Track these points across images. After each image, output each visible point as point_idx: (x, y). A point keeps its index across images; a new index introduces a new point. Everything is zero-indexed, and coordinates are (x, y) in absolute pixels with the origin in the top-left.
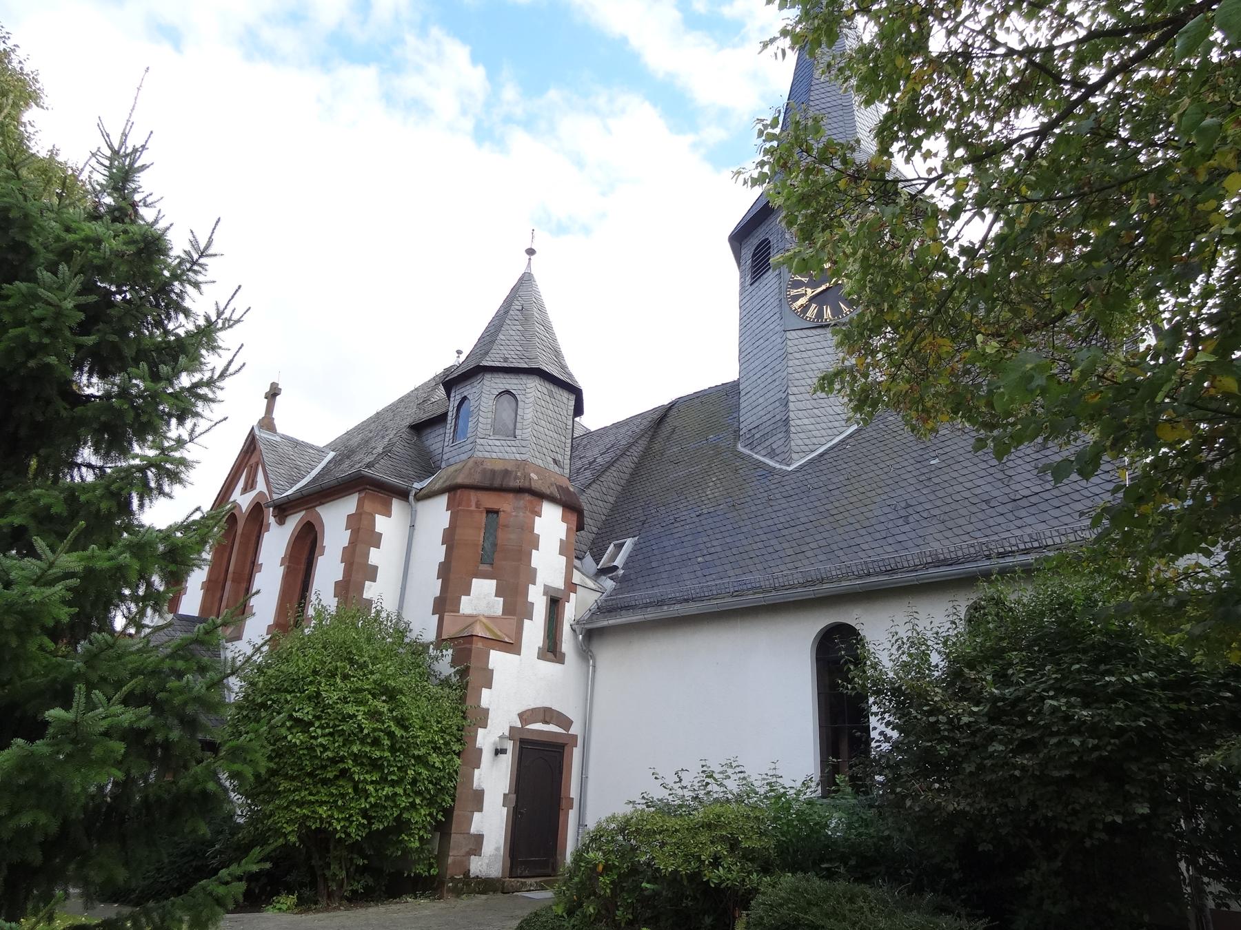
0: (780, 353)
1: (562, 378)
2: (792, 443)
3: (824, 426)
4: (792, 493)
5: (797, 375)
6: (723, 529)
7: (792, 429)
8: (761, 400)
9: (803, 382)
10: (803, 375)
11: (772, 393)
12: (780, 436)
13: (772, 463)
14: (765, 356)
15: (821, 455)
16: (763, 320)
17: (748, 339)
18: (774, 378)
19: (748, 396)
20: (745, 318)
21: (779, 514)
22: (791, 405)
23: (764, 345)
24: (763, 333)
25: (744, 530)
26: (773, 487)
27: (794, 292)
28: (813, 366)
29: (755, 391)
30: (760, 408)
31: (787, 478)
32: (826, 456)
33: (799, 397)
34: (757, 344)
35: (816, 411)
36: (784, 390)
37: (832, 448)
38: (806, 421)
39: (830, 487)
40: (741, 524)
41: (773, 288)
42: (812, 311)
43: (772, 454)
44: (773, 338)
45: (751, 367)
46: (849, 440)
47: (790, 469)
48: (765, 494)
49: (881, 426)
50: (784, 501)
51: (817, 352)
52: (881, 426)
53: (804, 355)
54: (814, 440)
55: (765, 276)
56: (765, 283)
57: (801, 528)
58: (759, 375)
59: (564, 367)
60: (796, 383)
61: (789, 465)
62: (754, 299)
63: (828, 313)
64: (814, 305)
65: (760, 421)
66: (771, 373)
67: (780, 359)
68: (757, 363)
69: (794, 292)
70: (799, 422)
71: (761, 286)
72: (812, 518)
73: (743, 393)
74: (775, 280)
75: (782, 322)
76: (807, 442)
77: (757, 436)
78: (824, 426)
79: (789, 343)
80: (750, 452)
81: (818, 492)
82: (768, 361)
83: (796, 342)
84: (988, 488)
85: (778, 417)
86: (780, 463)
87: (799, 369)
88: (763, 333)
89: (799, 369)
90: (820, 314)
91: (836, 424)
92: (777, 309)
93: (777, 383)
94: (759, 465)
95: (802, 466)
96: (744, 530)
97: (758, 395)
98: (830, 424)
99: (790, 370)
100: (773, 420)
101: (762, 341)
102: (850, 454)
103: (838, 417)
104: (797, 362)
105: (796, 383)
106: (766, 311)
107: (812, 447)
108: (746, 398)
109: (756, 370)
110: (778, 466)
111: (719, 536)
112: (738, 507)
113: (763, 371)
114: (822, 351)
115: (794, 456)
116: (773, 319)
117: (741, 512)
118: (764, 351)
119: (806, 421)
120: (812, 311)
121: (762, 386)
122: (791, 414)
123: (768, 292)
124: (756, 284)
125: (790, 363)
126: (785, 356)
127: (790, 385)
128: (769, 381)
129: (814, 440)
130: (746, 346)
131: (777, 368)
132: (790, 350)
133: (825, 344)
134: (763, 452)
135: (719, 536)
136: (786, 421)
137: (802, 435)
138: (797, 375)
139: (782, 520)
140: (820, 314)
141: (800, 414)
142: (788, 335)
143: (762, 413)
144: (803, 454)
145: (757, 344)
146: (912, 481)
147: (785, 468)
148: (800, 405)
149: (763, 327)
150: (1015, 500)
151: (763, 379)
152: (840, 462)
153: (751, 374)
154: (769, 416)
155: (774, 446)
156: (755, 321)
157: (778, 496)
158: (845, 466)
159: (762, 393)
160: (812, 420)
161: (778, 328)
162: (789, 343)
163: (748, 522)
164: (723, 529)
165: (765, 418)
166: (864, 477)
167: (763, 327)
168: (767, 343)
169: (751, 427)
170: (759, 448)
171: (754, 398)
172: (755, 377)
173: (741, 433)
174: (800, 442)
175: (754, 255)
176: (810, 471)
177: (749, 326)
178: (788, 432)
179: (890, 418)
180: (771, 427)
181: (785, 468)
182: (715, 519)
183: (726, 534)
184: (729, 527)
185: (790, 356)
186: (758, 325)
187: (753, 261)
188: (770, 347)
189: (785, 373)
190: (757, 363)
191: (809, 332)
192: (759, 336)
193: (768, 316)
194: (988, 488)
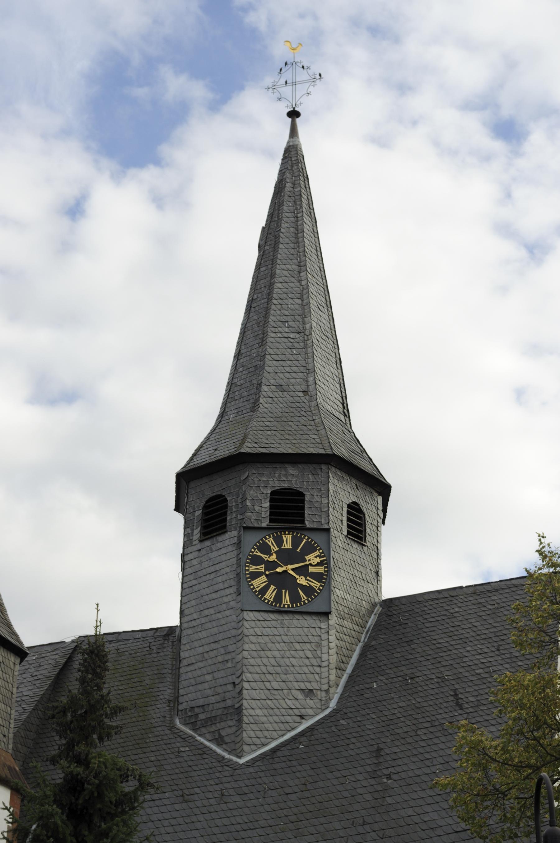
0: (234, 632)
1: (10, 639)
2: (244, 734)
3: (275, 718)
4: (246, 790)
5: (252, 661)
6: (173, 822)
7: (245, 718)
8: (208, 678)
9: (258, 669)
10: (259, 661)
11: (222, 674)
12: (230, 723)
13: (219, 751)
14: (216, 630)
15: (274, 751)
16: (216, 588)
17: (193, 603)
18: (227, 657)
19: (191, 668)
20: (191, 577)
21: (235, 813)
22: (245, 692)
23: (214, 617)
24: (214, 603)
25: (198, 825)
26: (224, 780)
27: (252, 569)
28: (269, 654)
29: (201, 665)
30: (206, 686)
31: (238, 772)
32: (279, 754)
33: (253, 685)
34: (206, 612)
35: (269, 702)
36: (238, 674)
37: (283, 745)
38: (259, 712)
39: (288, 790)
40: (194, 819)
41: (228, 556)
42: (270, 594)
43: (220, 741)
44: (228, 613)
45: (196, 636)
46: (303, 739)
47: (242, 761)
48: (217, 788)
49: (334, 729)
50: (237, 798)
51: (274, 639)
52: (334, 729)
53: (260, 640)
54: (266, 734)
55: (220, 538)
56: (219, 545)
57: (261, 832)
58: (207, 648)
59: (9, 625)
60: (251, 669)
61: (240, 757)
62: (203, 559)
63: (286, 599)
64: (272, 587)
65: (206, 701)
66: (222, 651)
67: (234, 640)
68: (204, 634)
69: (252, 569)
70: (252, 712)
71: (214, 548)
72: (271, 822)
73: (184, 662)
74: (230, 548)
75: (239, 598)
76: (259, 734)
77: (202, 716)
78: (275, 718)
79: (245, 623)
80: (191, 732)
81: (274, 793)
82: (221, 637)
83: (253, 624)
84: (435, 816)
85: (229, 703)
86: (230, 753)
87: (254, 654)
88: (214, 603)
89: (254, 654)
90: (278, 598)
91: (289, 719)
92: (233, 583)
93: (230, 665)
94: (204, 751)
95: (254, 760)
96: (198, 825)
97: (204, 671)
98: (282, 718)
99: (245, 654)
100: (222, 705)
101: (212, 611)
102: (304, 756)
103: (290, 712)
104: (253, 646)
105: (251, 669)
106: (220, 579)
107: (263, 740)
108: (188, 669)
109: (203, 641)
110: (227, 756)
111: (170, 830)
112: (186, 797)
113: (214, 646)
114: (278, 638)
115: (246, 748)
116: (227, 591)
117: (191, 805)
118: (214, 624)
119: (259, 712)
120: (270, 594)
121: (210, 662)
122: (245, 703)
123: (224, 558)
124: (207, 543)
125: (246, 647)
126: (240, 638)
127: (245, 671)
128: (220, 659)
129: (266, 734)
130: (192, 610)
131: (231, 648)
132: (246, 632)
133: (281, 631)
134: (207, 735)
135: (170, 830)
136: (239, 711)
137: (254, 727)
138: (252, 661)
139: (239, 820)
140: (278, 598)
141: (254, 704)
142: (246, 615)
143: (210, 692)
144: (254, 747)
145: (206, 612)
146: (368, 797)
147: (235, 759)
148: (254, 694)
149: (214, 596)
150: (457, 832)
151: (212, 654)
152: (295, 763)
153: (196, 644)
154: (218, 698)
155: (223, 733)
156: (204, 585)
157: (232, 792)
158: (300, 768)
159: (209, 669)
160: (265, 711)
161: (233, 604)
162: (245, 623)
163: (201, 818)
164: (173, 822)
165: (213, 699)
166: (321, 784)
167: (214, 596)
168: (219, 616)
169: (193, 704)
170: (204, 730)
171: (199, 672)
172: (201, 650)
173: (181, 707)
174: (252, 734)
175: (205, 507)
176: (263, 768)
177: (195, 588)
178: (240, 721)
179: (342, 722)
180: (220, 712)
181: (235, 759)
182: (163, 809)
183: (178, 828)
184: (181, 820)
185: (246, 639)
186: (208, 591)
187: (204, 514)
188: (223, 622)
189: (240, 656)
190: (204, 634)
191: (265, 615)
192: (209, 604)
193: (221, 586)
194: (435, 816)
